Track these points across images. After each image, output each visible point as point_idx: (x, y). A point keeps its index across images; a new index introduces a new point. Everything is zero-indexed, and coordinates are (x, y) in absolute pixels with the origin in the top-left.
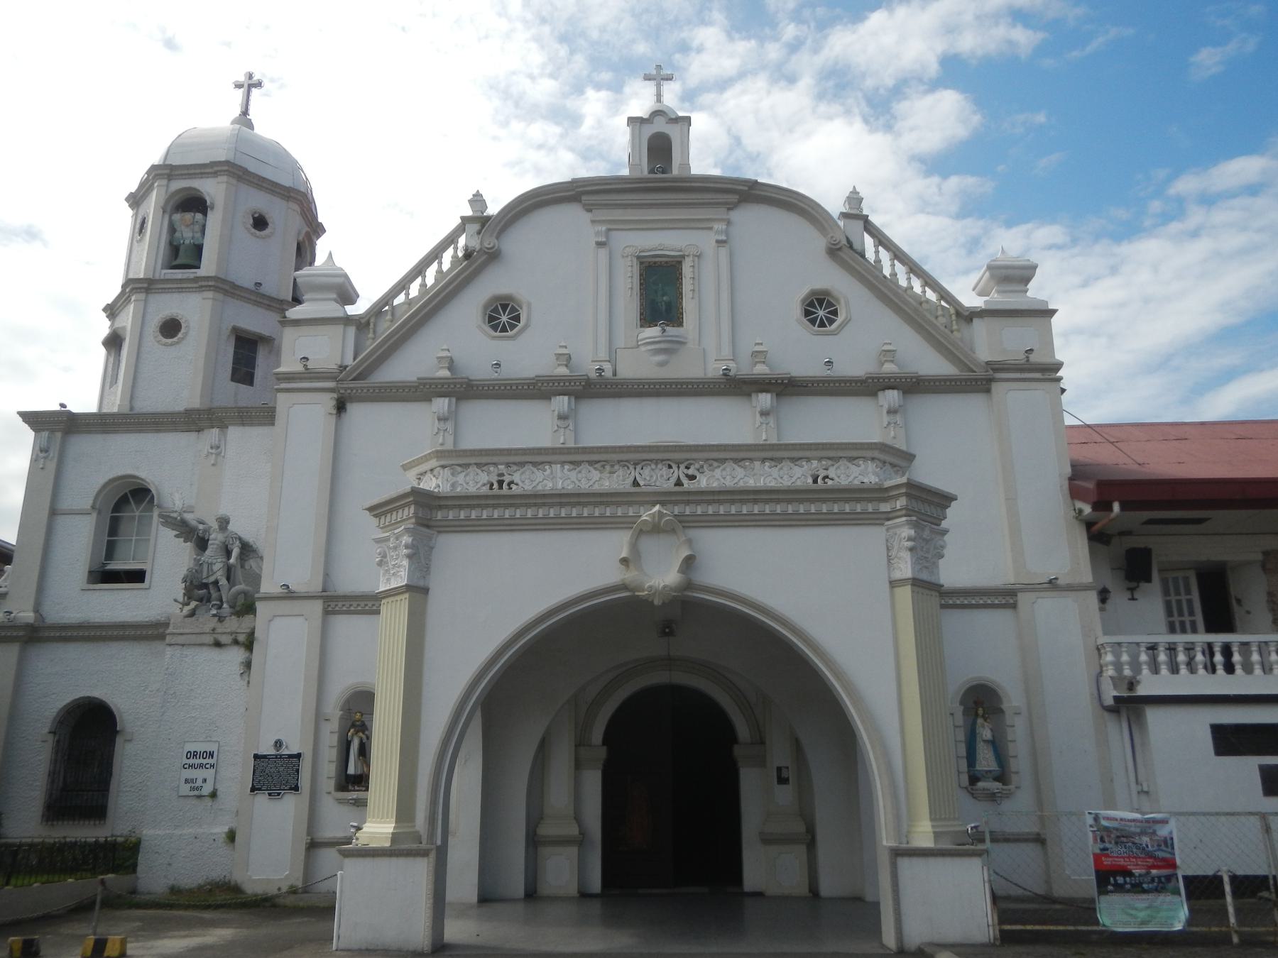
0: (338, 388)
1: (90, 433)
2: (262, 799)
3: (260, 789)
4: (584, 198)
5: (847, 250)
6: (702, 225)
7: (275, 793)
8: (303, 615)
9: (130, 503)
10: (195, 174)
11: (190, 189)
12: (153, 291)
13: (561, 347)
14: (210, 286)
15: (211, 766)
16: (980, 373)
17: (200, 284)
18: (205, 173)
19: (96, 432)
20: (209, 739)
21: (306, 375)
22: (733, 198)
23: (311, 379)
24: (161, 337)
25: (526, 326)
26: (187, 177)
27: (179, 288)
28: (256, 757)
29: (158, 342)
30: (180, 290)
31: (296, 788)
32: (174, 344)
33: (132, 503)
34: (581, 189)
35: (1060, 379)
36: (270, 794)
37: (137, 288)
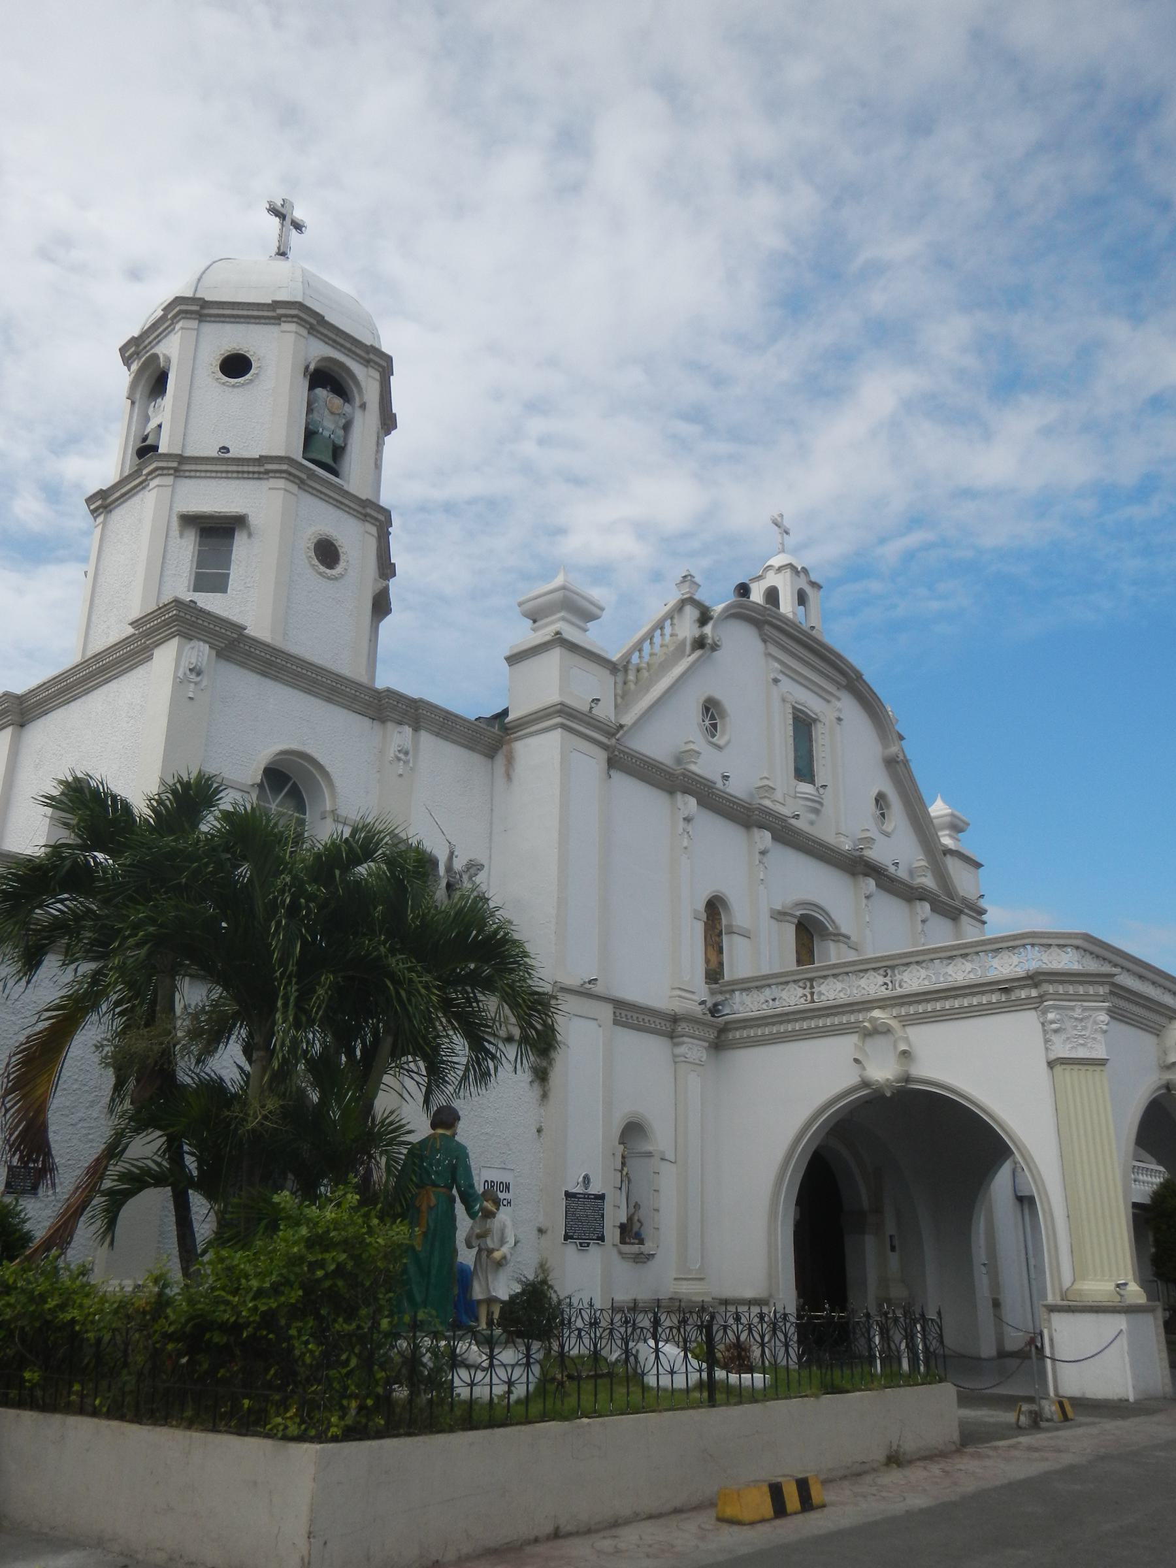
0: (615, 746)
1: (243, 667)
2: (571, 1250)
3: (572, 1238)
4: (767, 627)
5: (901, 764)
7: (583, 1246)
8: (596, 1020)
9: (281, 792)
10: (342, 346)
11: (342, 365)
12: (306, 488)
13: (761, 779)
14: (376, 519)
15: (508, 1203)
16: (957, 904)
17: (369, 510)
18: (354, 353)
19: (253, 670)
20: (504, 1166)
21: (587, 718)
22: (844, 682)
23: (589, 725)
24: (316, 562)
26: (330, 342)
27: (337, 501)
28: (568, 1195)
29: (310, 562)
30: (338, 504)
31: (602, 1238)
32: (332, 579)
33: (268, 792)
34: (770, 619)
35: (984, 923)
36: (581, 1244)
37: (290, 474)
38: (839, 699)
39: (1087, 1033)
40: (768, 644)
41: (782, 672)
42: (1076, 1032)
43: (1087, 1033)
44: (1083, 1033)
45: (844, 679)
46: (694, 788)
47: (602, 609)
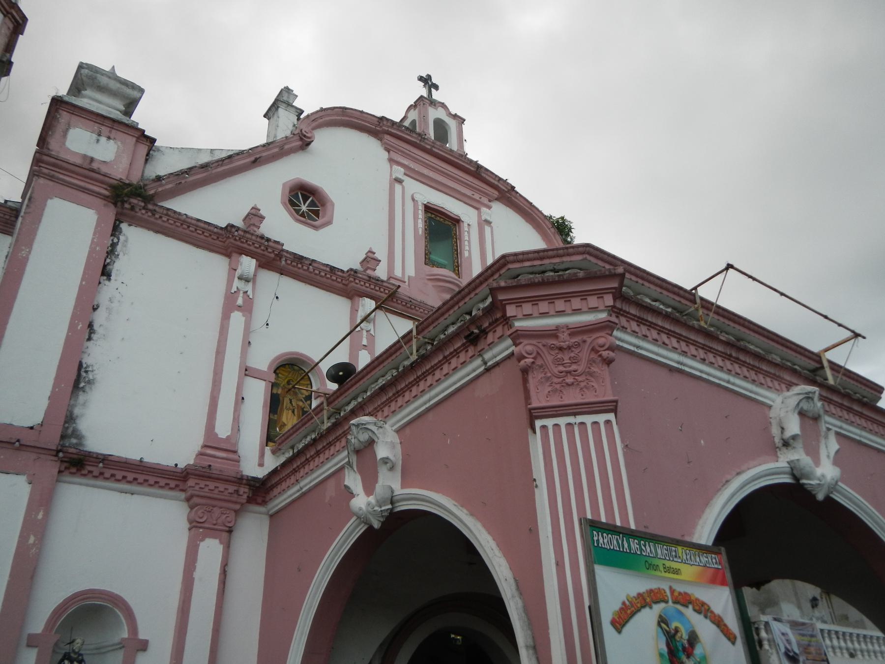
4: (387, 137)
6: (475, 205)
22: (496, 194)
25: (329, 223)
38: (489, 207)
39: (580, 368)
40: (391, 152)
41: (405, 174)
42: (561, 368)
43: (580, 368)
44: (574, 367)
45: (496, 193)
46: (252, 248)
47: (142, 91)
